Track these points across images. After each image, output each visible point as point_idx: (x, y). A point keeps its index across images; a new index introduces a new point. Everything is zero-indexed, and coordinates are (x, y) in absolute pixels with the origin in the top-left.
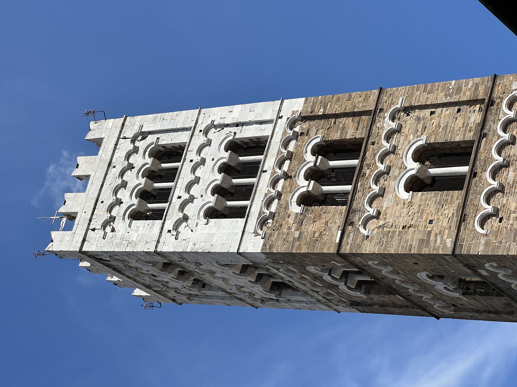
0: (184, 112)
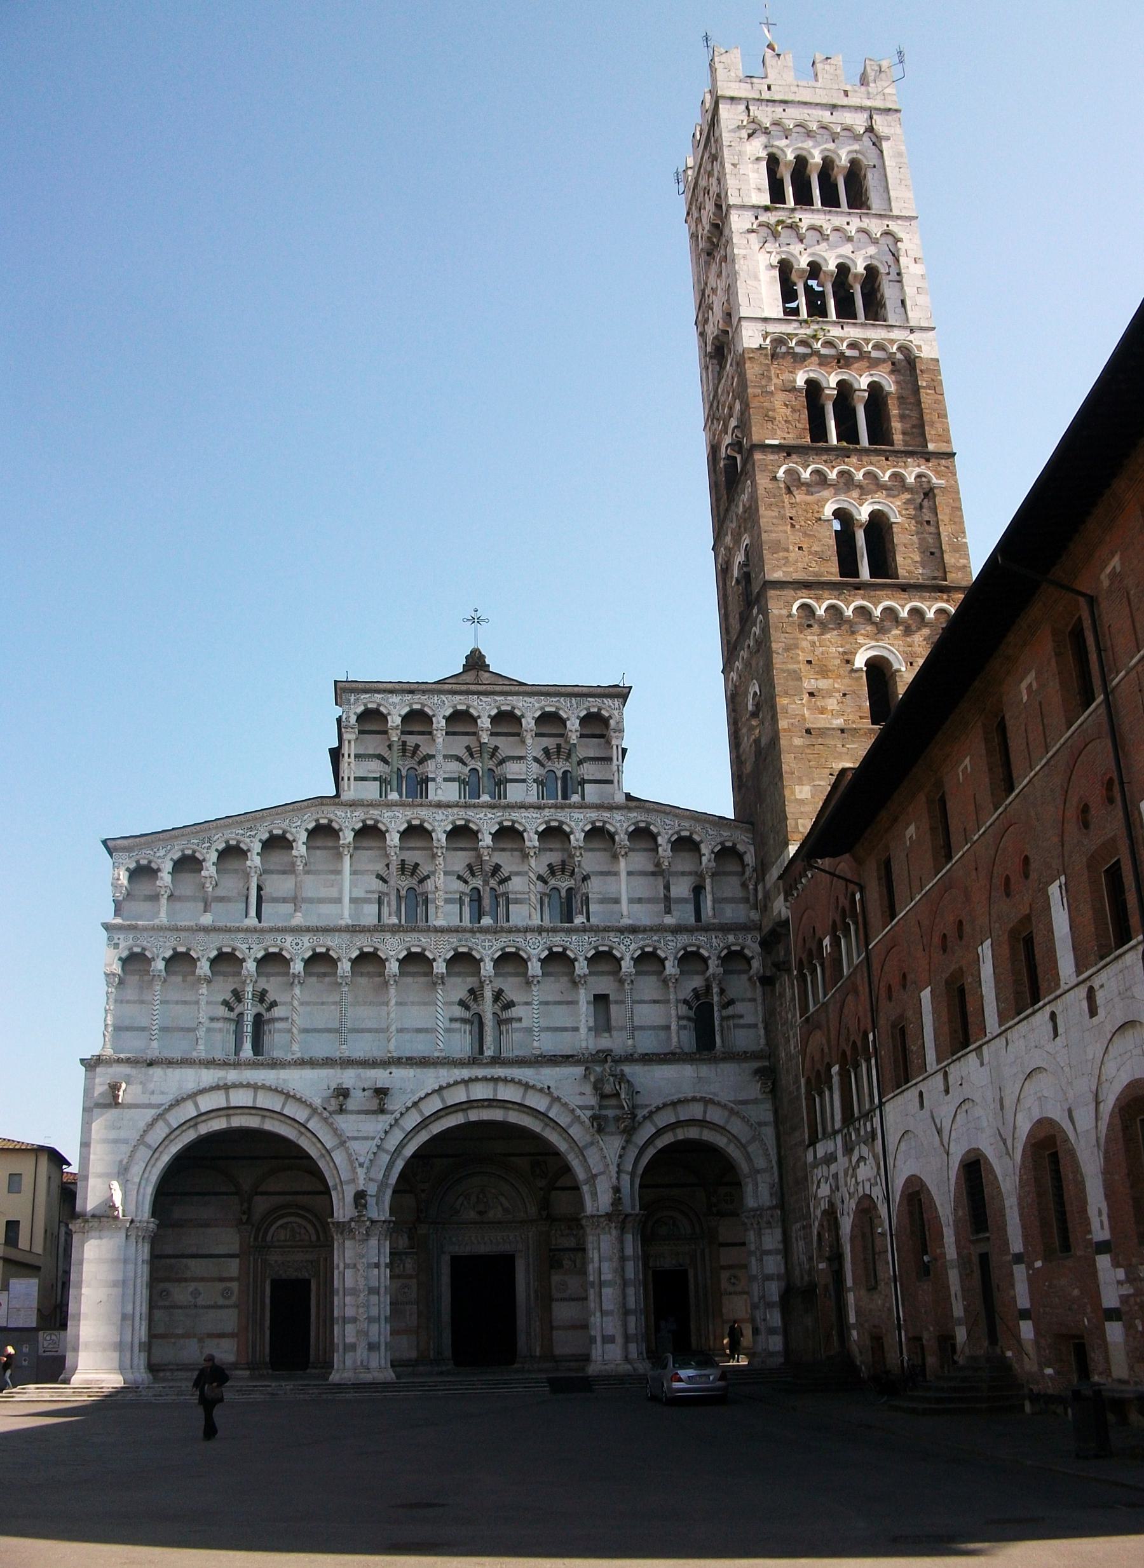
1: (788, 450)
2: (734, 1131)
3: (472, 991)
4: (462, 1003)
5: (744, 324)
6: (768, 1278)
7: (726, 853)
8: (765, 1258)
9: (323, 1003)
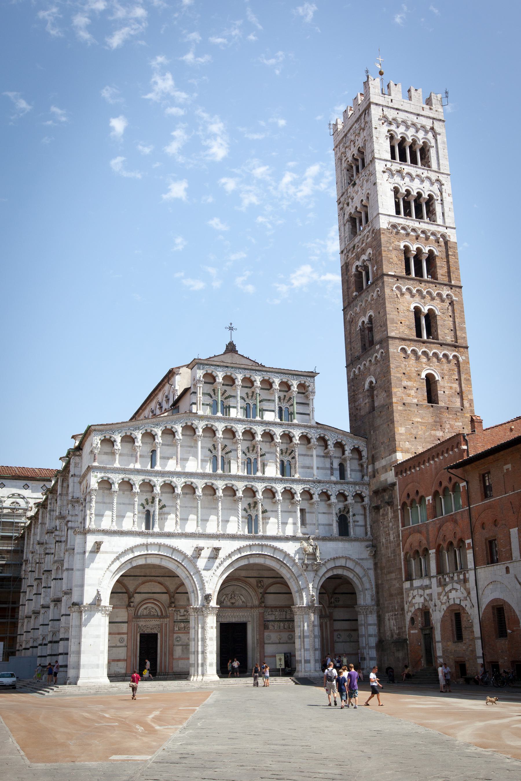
0: (448, 163)
1: (398, 278)
2: (357, 572)
3: (249, 504)
4: (245, 510)
5: (380, 216)
6: (370, 636)
7: (356, 450)
8: (369, 627)
9: (186, 507)
